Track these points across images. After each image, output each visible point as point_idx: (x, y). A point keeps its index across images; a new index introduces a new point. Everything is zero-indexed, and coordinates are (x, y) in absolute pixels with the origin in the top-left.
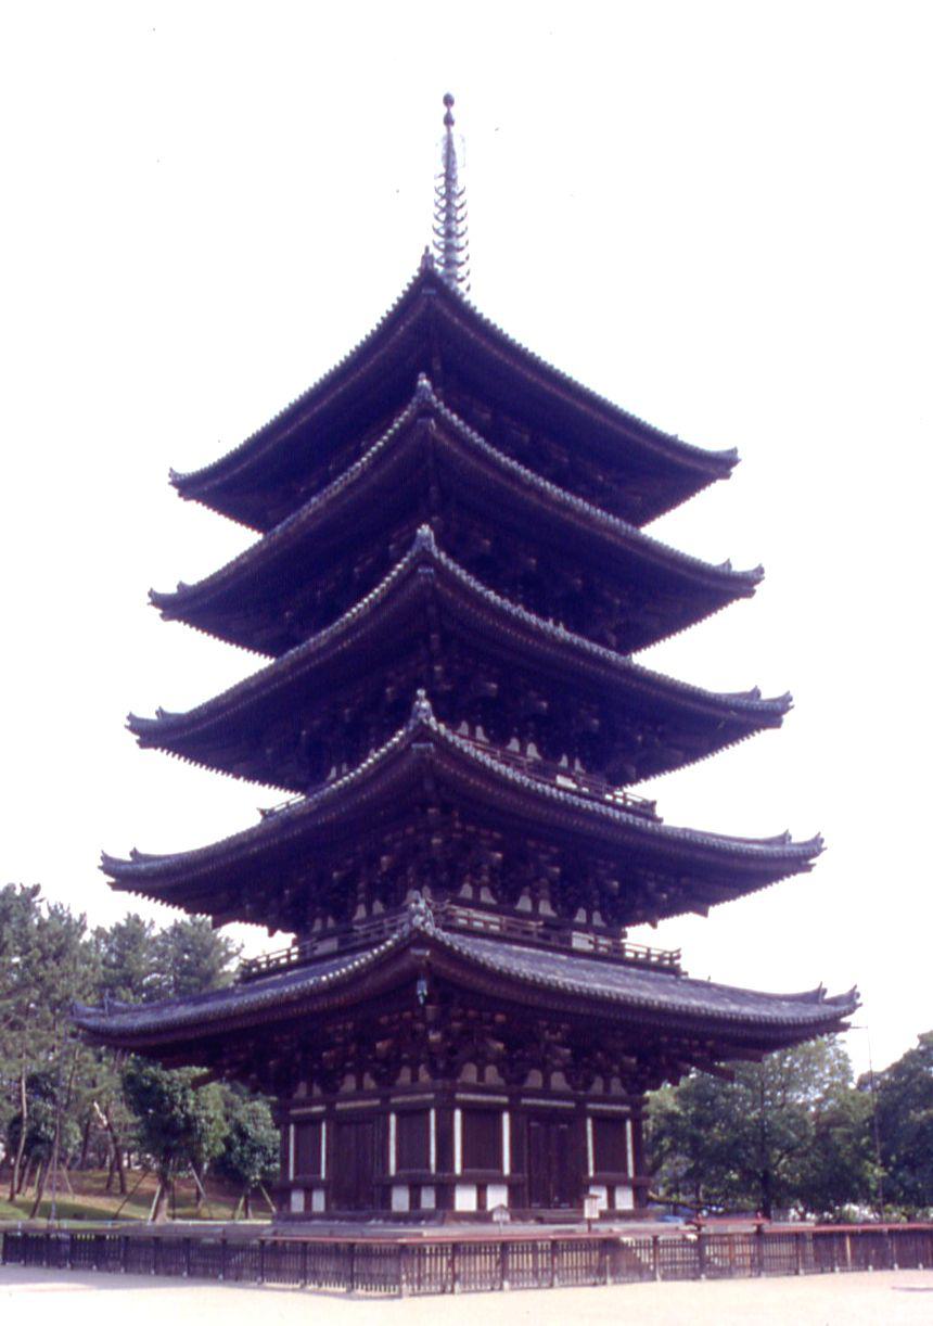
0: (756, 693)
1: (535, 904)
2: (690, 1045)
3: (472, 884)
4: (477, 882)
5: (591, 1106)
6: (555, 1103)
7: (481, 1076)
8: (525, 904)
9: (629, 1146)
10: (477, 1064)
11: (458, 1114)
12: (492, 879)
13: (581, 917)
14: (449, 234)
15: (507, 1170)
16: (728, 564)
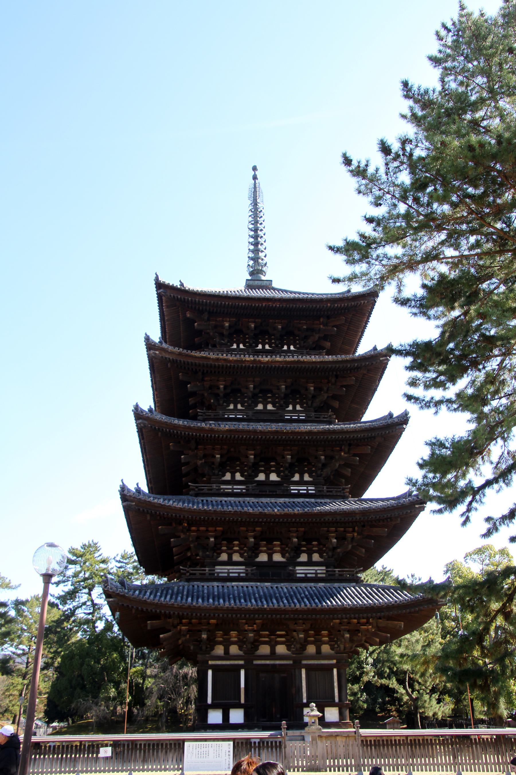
0: (391, 415)
1: (270, 556)
2: (358, 623)
3: (227, 553)
4: (229, 551)
5: (304, 662)
6: (278, 662)
7: (227, 651)
8: (263, 558)
9: (336, 684)
10: (223, 645)
11: (210, 672)
12: (241, 549)
13: (304, 558)
14: (256, 230)
15: (243, 701)
16: (375, 348)
